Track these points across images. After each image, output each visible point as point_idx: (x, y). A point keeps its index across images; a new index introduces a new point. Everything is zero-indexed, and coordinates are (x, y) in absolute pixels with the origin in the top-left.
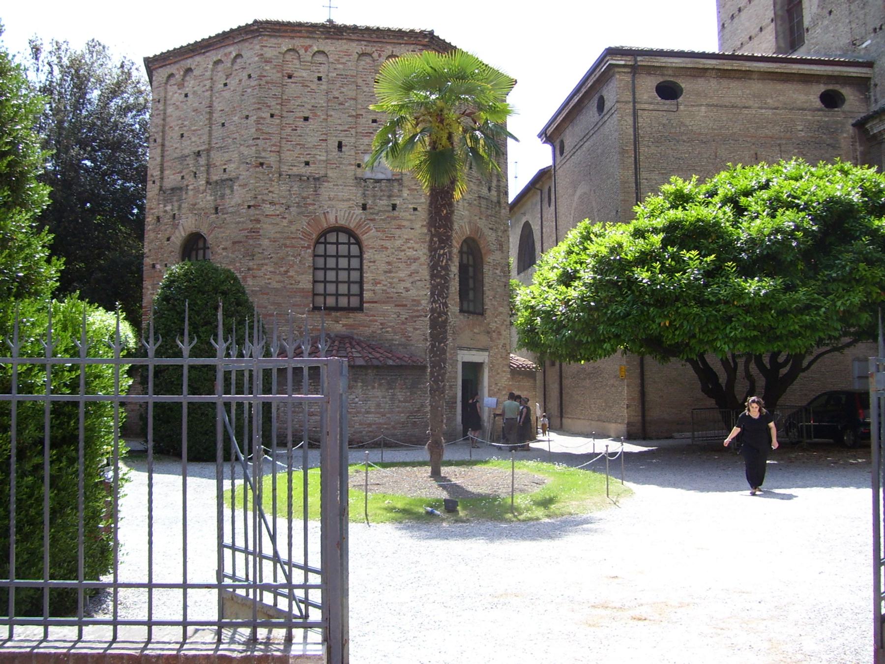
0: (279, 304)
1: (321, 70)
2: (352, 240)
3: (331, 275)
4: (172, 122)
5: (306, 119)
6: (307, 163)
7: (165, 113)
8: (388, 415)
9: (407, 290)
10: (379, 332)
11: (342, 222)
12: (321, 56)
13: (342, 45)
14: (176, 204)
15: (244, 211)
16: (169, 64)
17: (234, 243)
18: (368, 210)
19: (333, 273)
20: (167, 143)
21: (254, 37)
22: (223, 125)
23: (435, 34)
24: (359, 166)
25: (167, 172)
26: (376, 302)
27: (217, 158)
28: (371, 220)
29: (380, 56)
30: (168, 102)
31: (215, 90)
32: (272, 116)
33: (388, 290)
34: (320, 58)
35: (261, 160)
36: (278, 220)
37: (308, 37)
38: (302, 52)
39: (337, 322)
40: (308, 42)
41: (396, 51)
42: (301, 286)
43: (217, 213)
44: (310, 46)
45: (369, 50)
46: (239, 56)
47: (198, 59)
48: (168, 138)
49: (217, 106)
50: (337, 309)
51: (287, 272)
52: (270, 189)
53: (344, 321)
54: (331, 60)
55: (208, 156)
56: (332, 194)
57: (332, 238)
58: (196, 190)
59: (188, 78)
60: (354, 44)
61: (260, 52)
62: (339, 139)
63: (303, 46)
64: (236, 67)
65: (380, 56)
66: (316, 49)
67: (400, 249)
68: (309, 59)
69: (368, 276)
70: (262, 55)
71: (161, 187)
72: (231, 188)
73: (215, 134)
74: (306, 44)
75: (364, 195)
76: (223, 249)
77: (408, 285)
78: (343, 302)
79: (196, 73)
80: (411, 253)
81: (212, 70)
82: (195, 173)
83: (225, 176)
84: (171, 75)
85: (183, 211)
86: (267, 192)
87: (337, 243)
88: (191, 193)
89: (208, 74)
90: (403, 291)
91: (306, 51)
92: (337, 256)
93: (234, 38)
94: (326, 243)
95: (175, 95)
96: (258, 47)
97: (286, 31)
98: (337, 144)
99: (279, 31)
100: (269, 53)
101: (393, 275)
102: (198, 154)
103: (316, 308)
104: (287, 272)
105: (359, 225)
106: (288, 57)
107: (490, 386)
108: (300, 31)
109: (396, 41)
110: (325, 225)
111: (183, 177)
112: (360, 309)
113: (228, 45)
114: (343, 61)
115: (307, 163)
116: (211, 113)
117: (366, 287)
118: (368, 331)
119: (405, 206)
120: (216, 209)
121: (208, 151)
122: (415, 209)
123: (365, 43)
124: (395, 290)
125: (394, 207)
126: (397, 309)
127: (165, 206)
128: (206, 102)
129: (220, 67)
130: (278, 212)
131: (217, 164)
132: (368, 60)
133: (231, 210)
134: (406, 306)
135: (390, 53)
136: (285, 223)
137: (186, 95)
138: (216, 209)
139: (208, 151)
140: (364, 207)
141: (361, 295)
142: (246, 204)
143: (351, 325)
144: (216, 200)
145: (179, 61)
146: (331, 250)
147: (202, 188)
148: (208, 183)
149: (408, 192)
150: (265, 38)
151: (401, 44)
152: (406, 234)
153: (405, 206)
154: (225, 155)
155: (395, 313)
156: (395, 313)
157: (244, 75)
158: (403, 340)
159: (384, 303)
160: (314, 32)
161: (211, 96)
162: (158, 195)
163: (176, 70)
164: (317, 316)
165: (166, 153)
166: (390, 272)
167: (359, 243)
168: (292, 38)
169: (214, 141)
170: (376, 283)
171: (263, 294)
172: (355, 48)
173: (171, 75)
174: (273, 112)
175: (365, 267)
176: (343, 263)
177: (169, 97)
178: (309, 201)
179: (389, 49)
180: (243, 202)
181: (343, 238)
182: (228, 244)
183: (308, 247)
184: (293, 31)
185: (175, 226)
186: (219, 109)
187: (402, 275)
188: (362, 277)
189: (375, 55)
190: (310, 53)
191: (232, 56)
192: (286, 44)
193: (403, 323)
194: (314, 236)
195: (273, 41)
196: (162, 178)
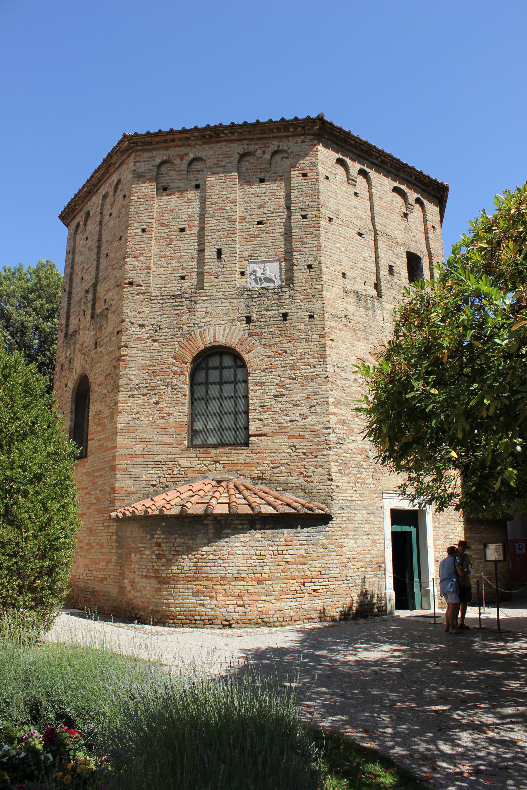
0: (147, 442)
1: (199, 177)
2: (239, 363)
3: (214, 406)
4: (77, 269)
5: (182, 230)
6: (183, 278)
7: (73, 262)
8: (267, 582)
9: (303, 416)
10: (269, 473)
11: (221, 340)
12: (200, 163)
13: (222, 148)
14: (72, 348)
15: (114, 338)
16: (77, 214)
17: (106, 376)
18: (252, 324)
19: (217, 403)
20: (74, 291)
21: (129, 156)
22: (107, 255)
23: (327, 118)
24: (243, 274)
25: (71, 319)
26: (265, 435)
27: (101, 289)
28: (257, 334)
29: (264, 153)
30: (76, 251)
31: (104, 222)
32: (144, 230)
33: (281, 419)
34: (197, 166)
35: (131, 280)
36: (149, 342)
37: (183, 145)
38: (177, 161)
39: (217, 462)
40: (184, 150)
41: (284, 145)
42: (172, 419)
43: (96, 348)
44: (187, 154)
45: (251, 148)
46: (119, 181)
47: (94, 199)
48: (74, 285)
49: (104, 238)
50: (221, 445)
51: (157, 403)
52: (139, 310)
53: (225, 460)
54: (209, 165)
55: (95, 290)
56: (209, 310)
57: (215, 362)
58: (84, 328)
59: (89, 222)
60: (235, 145)
61: (133, 168)
62: (217, 247)
63: (178, 156)
64: (118, 194)
65: (264, 153)
66: (192, 156)
67: (293, 368)
68: (185, 167)
69: (254, 401)
70: (135, 170)
71: (66, 335)
72: (107, 316)
73: (102, 267)
74: (182, 153)
75: (248, 306)
76: (99, 385)
77: (306, 411)
78: (229, 436)
79: (92, 213)
80: (309, 371)
81: (102, 205)
82: (85, 312)
83: (106, 307)
84: (78, 225)
85: (77, 352)
86: (136, 313)
87: (221, 368)
88: (81, 332)
89: (98, 210)
90: (299, 419)
91: (181, 160)
92: (221, 383)
93: (115, 164)
94: (208, 369)
95: (81, 243)
96: (132, 164)
97: (157, 143)
98: (216, 253)
99: (150, 143)
100: (142, 168)
101: (284, 399)
102: (87, 291)
103: (192, 445)
104: (157, 403)
105: (242, 341)
106: (164, 169)
107: (435, 540)
108: (173, 140)
109: (281, 134)
110: (202, 347)
111: (79, 320)
112: (247, 444)
113: (112, 174)
114: (223, 163)
115: (183, 278)
116: (99, 247)
117: (252, 416)
118: (255, 472)
119: (298, 315)
120: (96, 343)
121: (95, 285)
122: (311, 317)
123: (247, 142)
124: (288, 419)
125: (285, 316)
126: (292, 442)
127: (66, 352)
128: (96, 238)
129: (109, 200)
130: (148, 335)
131: (101, 296)
132: (252, 159)
133: (106, 340)
134: (303, 437)
135: (276, 148)
136: (156, 344)
137: (87, 239)
138: (96, 343)
139: (95, 285)
140: (249, 320)
141: (247, 428)
142: (116, 331)
143: (235, 465)
144: (96, 334)
145: (83, 207)
146: (214, 376)
147: (88, 324)
148: (92, 317)
149: (301, 297)
150: (139, 154)
151: (288, 137)
152: (300, 348)
153: (298, 315)
154: (106, 285)
155: (290, 447)
156: (290, 447)
157: (121, 197)
158: (301, 481)
159: (275, 435)
160: (188, 139)
161: (100, 230)
162: (63, 342)
163: (80, 218)
164: (192, 455)
165: (72, 300)
166: (283, 396)
167: (244, 365)
168: (167, 149)
169: (101, 274)
170: (264, 409)
171: (129, 431)
172: (237, 149)
173: (78, 225)
174: (144, 227)
175: (251, 394)
176: (228, 390)
177: (77, 246)
178: (184, 318)
179: (274, 145)
180: (114, 328)
181: (228, 361)
182: (101, 378)
183: (182, 373)
184: (166, 141)
185: (71, 369)
186: (106, 240)
187: (295, 397)
188: (248, 404)
189: (259, 153)
190: (186, 162)
191: (114, 184)
192: (159, 156)
193: (300, 459)
194: (189, 359)
195: (147, 154)
196: (67, 325)
